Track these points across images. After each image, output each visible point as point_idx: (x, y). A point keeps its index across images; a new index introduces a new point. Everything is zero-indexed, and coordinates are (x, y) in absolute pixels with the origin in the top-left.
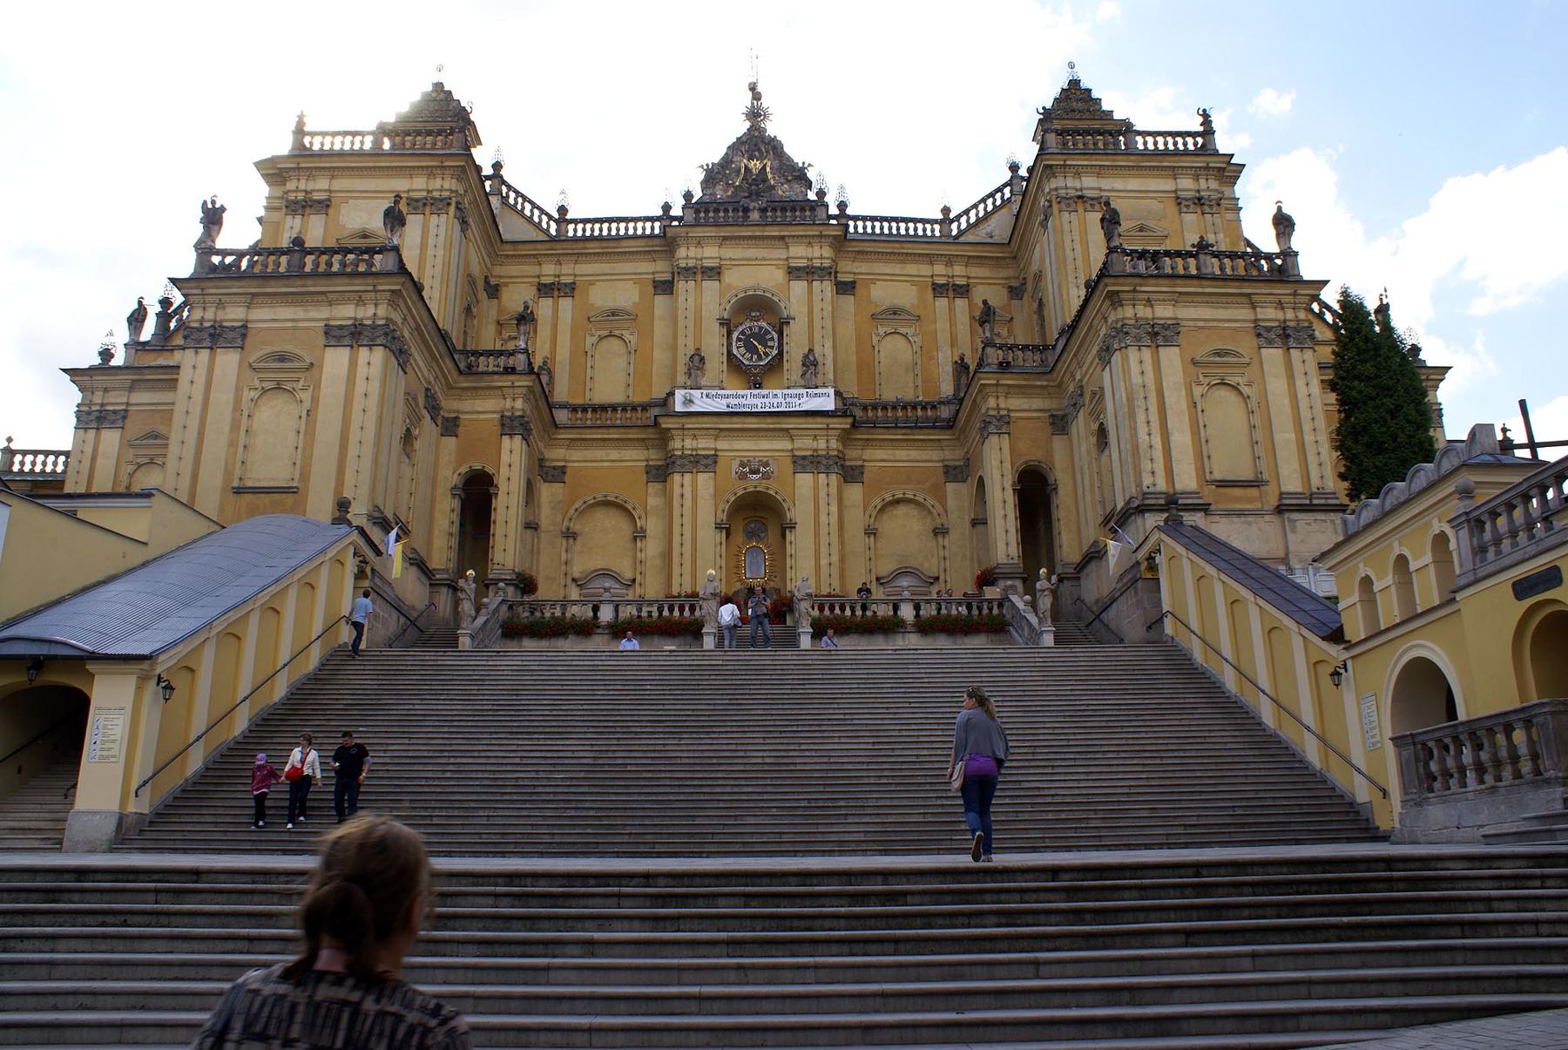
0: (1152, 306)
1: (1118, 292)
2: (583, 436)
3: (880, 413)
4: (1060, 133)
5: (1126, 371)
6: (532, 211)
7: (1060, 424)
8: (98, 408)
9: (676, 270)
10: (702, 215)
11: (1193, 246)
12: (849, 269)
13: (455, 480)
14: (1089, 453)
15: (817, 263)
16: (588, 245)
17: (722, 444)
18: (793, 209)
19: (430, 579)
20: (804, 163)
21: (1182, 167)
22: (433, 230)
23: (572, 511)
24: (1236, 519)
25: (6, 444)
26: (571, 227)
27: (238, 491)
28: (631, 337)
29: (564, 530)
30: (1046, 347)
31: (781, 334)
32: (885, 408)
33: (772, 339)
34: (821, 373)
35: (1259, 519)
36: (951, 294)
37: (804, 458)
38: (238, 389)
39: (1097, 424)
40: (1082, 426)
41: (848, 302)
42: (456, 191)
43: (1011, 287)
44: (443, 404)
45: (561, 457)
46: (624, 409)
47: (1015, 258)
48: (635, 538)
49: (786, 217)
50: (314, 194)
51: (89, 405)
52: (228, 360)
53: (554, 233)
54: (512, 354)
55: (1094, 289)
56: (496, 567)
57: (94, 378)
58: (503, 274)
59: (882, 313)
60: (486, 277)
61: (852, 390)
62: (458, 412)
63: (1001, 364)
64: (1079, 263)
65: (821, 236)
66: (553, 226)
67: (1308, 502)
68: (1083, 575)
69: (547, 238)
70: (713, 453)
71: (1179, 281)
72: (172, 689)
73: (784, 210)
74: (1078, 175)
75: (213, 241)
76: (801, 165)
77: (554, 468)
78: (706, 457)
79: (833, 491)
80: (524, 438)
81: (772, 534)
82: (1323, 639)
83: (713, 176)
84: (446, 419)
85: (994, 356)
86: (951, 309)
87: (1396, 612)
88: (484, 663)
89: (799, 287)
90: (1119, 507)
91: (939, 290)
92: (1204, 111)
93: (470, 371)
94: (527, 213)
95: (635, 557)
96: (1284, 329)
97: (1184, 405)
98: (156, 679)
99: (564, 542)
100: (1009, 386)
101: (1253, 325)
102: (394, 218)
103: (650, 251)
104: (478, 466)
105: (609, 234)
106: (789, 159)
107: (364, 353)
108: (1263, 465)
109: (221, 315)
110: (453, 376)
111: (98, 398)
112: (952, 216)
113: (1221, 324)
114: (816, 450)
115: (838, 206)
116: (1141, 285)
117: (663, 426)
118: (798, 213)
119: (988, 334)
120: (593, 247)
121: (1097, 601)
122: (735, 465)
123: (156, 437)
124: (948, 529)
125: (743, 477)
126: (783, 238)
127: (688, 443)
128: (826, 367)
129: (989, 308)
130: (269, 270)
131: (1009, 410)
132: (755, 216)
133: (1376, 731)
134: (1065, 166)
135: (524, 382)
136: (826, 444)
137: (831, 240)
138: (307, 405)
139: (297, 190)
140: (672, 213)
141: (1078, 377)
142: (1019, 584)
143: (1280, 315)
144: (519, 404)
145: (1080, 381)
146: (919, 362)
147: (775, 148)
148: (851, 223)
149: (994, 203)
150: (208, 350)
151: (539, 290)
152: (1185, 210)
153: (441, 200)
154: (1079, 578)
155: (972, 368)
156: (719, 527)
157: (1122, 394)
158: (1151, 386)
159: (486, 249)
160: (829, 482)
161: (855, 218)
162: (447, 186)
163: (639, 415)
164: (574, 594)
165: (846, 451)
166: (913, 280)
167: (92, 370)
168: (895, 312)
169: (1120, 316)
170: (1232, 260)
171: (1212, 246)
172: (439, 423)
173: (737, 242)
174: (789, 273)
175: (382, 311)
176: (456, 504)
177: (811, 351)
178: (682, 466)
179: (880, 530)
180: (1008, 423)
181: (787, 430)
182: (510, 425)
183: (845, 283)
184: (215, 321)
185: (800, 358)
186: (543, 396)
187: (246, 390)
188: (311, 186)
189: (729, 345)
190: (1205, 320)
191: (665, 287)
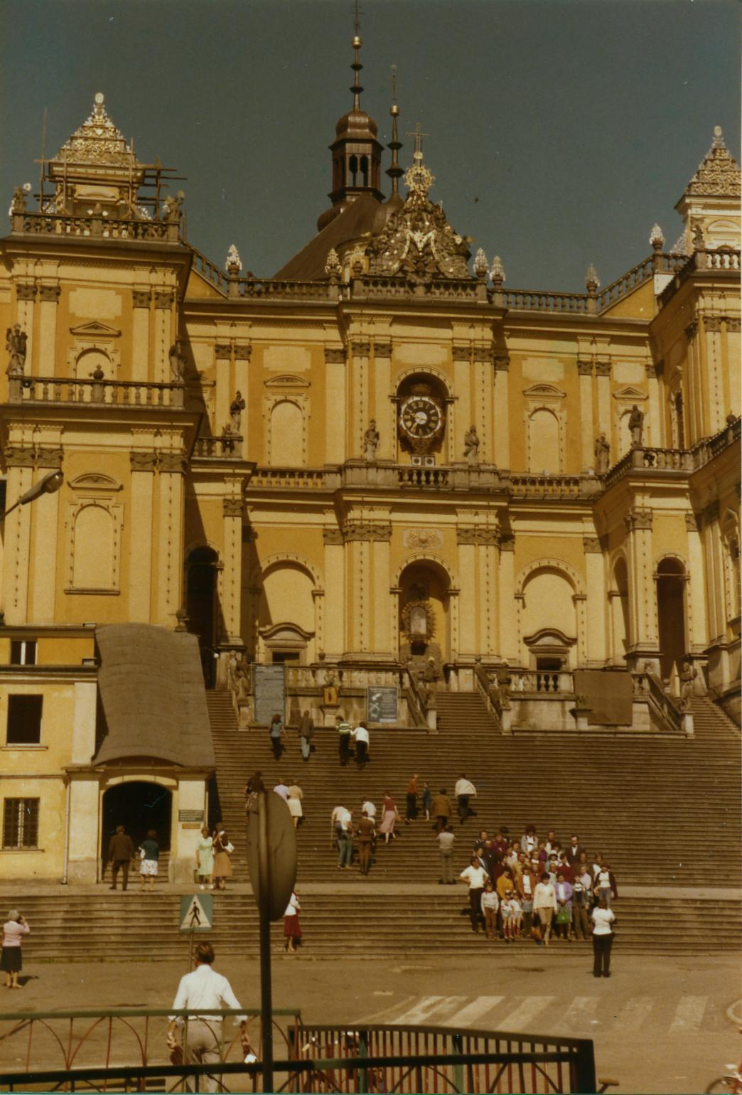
15: (478, 345)
17: (397, 516)
27: (69, 592)
36: (594, 371)
37: (467, 531)
70: (387, 523)
78: (383, 528)
91: (584, 367)
114: (476, 525)
124: (586, 596)
131: (652, 509)
132: (420, 291)
138: (120, 520)
168: (543, 388)
177: (473, 431)
178: (362, 535)
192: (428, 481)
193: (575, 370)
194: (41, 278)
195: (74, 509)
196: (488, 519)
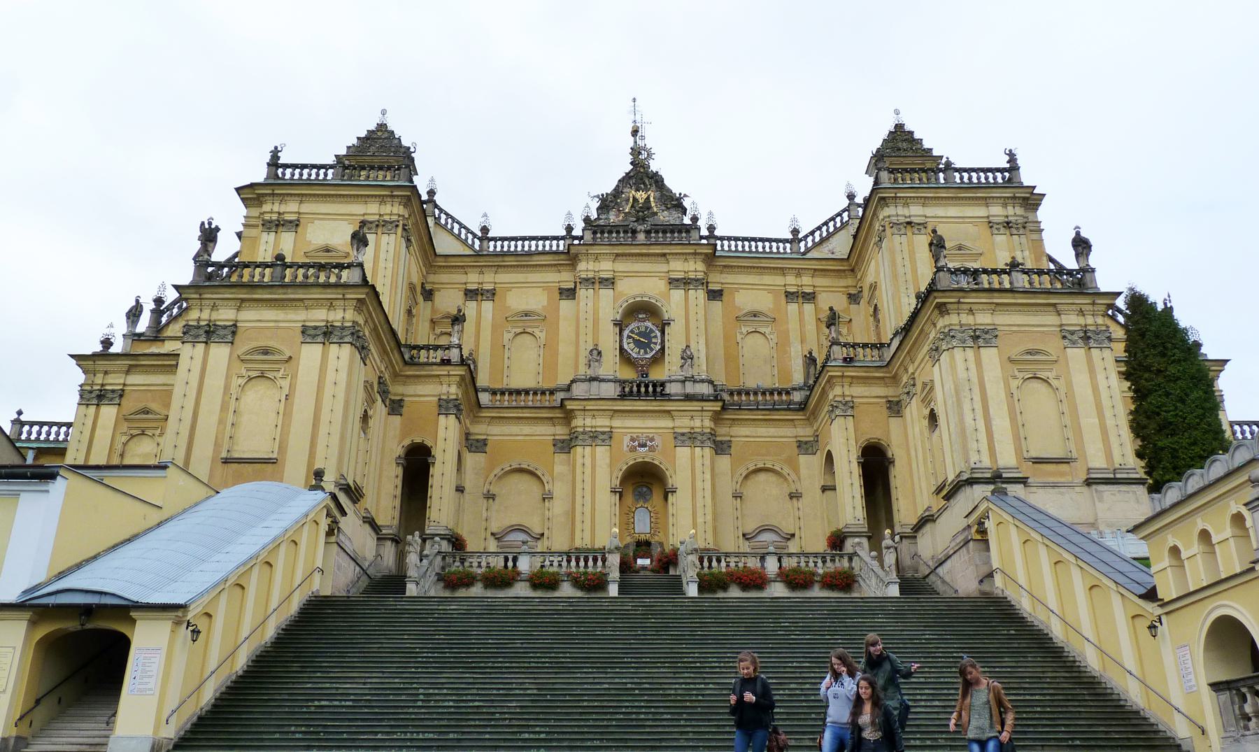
0: (973, 314)
1: (945, 304)
2: (502, 415)
3: (744, 398)
4: (891, 171)
5: (953, 367)
6: (460, 230)
7: (895, 407)
8: (99, 387)
9: (578, 280)
10: (599, 235)
11: (1007, 265)
12: (717, 280)
13: (399, 451)
14: (922, 433)
15: (692, 276)
16: (506, 259)
17: (617, 423)
18: (672, 232)
19: (377, 534)
20: (680, 194)
21: (993, 197)
22: (383, 247)
23: (492, 475)
24: (1051, 490)
25: (16, 416)
26: (492, 243)
27: (226, 461)
28: (540, 334)
29: (485, 492)
30: (882, 345)
31: (663, 332)
32: (748, 393)
33: (656, 337)
34: (696, 365)
35: (1070, 490)
36: (800, 300)
37: (683, 434)
38: (228, 377)
39: (929, 410)
40: (915, 412)
41: (717, 306)
42: (403, 216)
43: (849, 294)
44: (391, 389)
45: (484, 432)
46: (535, 393)
47: (852, 270)
48: (544, 499)
49: (667, 237)
50: (286, 215)
51: (92, 385)
52: (220, 353)
53: (478, 249)
54: (448, 348)
55: (924, 302)
56: (432, 524)
57: (97, 362)
58: (436, 281)
59: (745, 315)
60: (423, 284)
61: (720, 379)
62: (403, 395)
63: (845, 359)
64: (909, 277)
65: (695, 254)
66: (477, 242)
67: (1112, 476)
68: (919, 535)
69: (472, 253)
70: (608, 429)
71: (996, 295)
72: (199, 632)
73: (664, 232)
74: (906, 205)
75: (210, 256)
76: (678, 195)
77: (477, 440)
78: (603, 433)
79: (707, 462)
80: (457, 417)
81: (657, 497)
82: (1141, 597)
83: (606, 203)
84: (393, 401)
85: (839, 352)
86: (801, 313)
87: (1203, 577)
88: (436, 607)
89: (678, 295)
90: (950, 480)
91: (791, 297)
92: (1010, 151)
93: (412, 363)
94: (456, 231)
95: (544, 515)
96: (1085, 332)
97: (1003, 395)
98: (186, 624)
99: (485, 501)
100: (852, 377)
101: (1059, 329)
102: (359, 239)
103: (555, 265)
104: (418, 440)
105: (523, 250)
106: (670, 191)
107: (334, 348)
108: (1073, 447)
109: (215, 316)
110: (398, 365)
111: (99, 379)
112: (800, 236)
113: (1031, 329)
114: (693, 428)
115: (708, 229)
116: (964, 298)
117: (568, 407)
118: (676, 235)
119: (834, 335)
120: (510, 261)
121: (933, 557)
122: (627, 440)
123: (148, 413)
124: (801, 493)
125: (633, 449)
126: (664, 255)
127: (589, 422)
128: (700, 360)
129: (835, 313)
130: (256, 280)
131: (852, 397)
132: (641, 237)
133: (1192, 677)
134: (896, 197)
135: (461, 371)
136: (702, 423)
137: (703, 257)
139: (271, 212)
140: (574, 233)
141: (911, 370)
142: (865, 541)
143: (1081, 321)
144: (453, 389)
145: (913, 374)
146: (775, 356)
147: (656, 182)
148: (719, 242)
149: (835, 226)
150: (204, 344)
151: (466, 294)
152: (996, 232)
153: (391, 223)
154: (916, 537)
155: (819, 363)
156: (614, 492)
157: (949, 386)
158: (975, 380)
159: (423, 261)
160: (704, 454)
161: (722, 239)
162: (395, 211)
163: (547, 397)
164: (492, 546)
165: (716, 429)
166: (769, 289)
167: (95, 356)
169: (947, 323)
170: (1039, 276)
171: (1022, 264)
172: (387, 404)
173: (628, 258)
174: (670, 283)
175: (350, 315)
176: (400, 471)
177: (688, 346)
179: (745, 493)
180: (852, 407)
181: (669, 412)
182: (445, 406)
183: (714, 291)
184: (210, 321)
185: (679, 353)
186: (470, 381)
187: (235, 378)
188: (283, 208)
189: (621, 341)
190: (1018, 325)
191: (569, 293)
192: (647, 391)
193: (783, 296)
194: (284, 213)
195: (241, 381)
196: (702, 423)
